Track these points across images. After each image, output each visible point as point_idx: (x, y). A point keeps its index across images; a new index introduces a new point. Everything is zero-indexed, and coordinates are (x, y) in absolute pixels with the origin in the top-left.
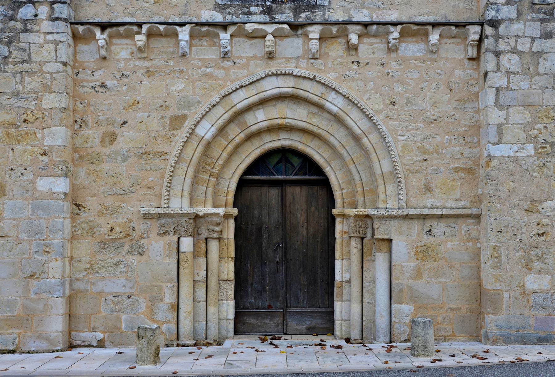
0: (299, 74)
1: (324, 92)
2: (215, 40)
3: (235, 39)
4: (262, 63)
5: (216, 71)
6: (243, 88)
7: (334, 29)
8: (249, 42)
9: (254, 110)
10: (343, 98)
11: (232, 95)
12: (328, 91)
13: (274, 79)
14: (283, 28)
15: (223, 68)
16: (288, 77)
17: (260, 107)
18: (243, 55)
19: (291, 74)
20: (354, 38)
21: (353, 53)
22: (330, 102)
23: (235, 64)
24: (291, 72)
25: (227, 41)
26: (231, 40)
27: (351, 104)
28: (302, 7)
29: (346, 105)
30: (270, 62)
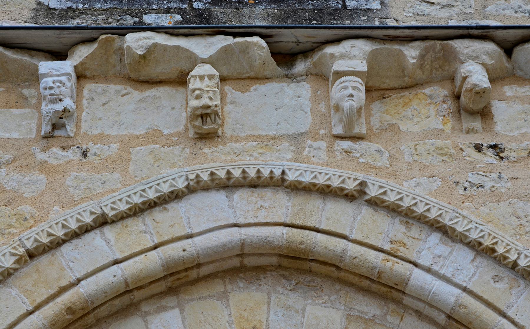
0: (307, 179)
1: (399, 237)
2: (26, 92)
3: (89, 87)
4: (180, 152)
5: (16, 176)
6: (107, 229)
7: (411, 53)
8: (136, 94)
9: (147, 313)
10: (469, 254)
11: (66, 249)
12: (415, 230)
13: (219, 198)
14: (245, 49)
15: (44, 167)
16: (268, 193)
17: (170, 301)
19: (279, 183)
20: (476, 75)
21: (477, 124)
22: (428, 270)
23: (85, 155)
24: (277, 173)
25: (64, 79)
26: (79, 87)
27: (505, 273)
28: (301, 13)
29: (488, 277)
30: (206, 150)
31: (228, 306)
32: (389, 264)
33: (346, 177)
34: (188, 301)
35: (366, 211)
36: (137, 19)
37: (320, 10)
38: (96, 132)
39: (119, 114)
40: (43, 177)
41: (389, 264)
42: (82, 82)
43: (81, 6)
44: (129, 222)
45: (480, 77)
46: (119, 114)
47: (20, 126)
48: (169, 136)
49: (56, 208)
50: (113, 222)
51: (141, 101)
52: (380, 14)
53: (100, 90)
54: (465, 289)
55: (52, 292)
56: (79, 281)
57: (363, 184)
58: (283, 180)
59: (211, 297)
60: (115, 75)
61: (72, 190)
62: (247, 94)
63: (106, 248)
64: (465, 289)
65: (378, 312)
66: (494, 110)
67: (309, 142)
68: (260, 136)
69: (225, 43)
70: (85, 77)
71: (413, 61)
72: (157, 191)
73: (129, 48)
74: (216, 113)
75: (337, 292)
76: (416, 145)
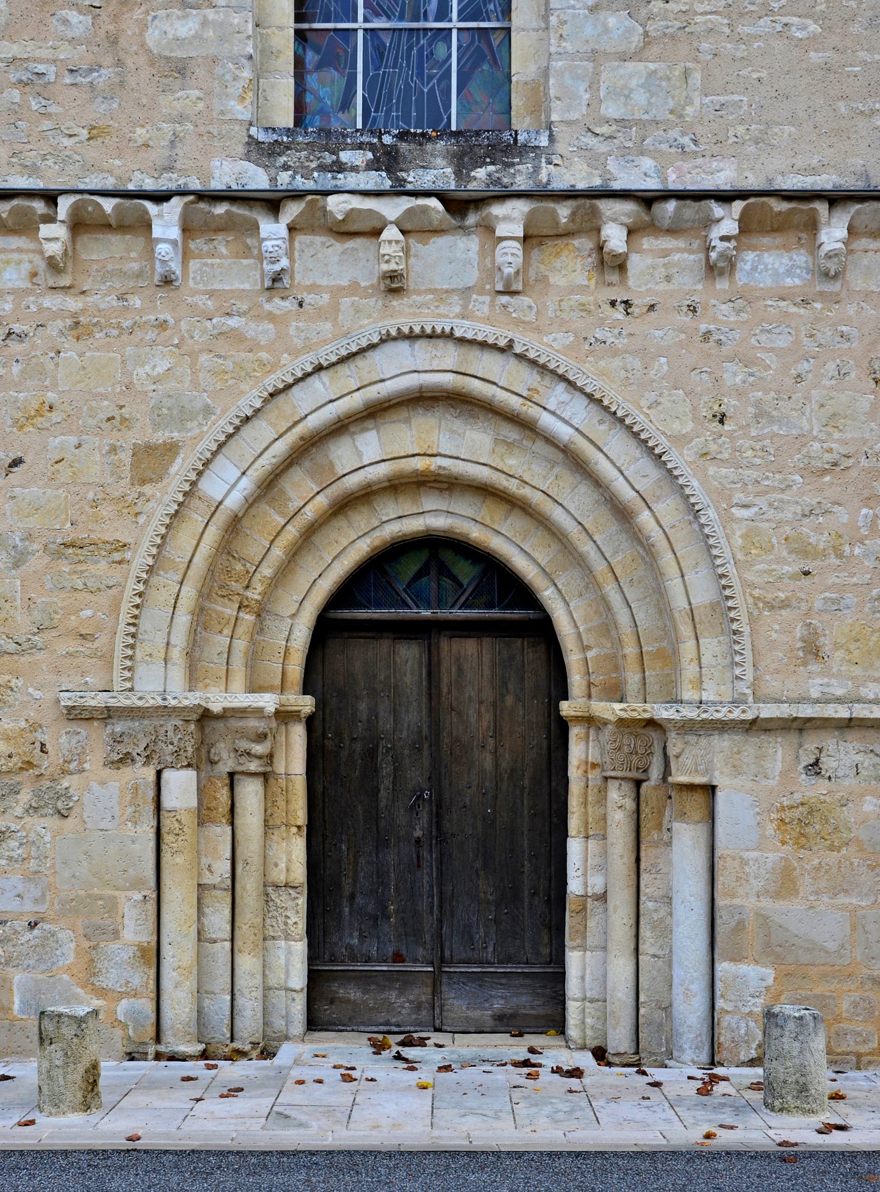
0: (469, 336)
1: (535, 385)
2: (249, 241)
3: (301, 239)
4: (374, 303)
5: (253, 325)
6: (323, 374)
7: (564, 211)
8: (339, 246)
9: (354, 433)
10: (585, 401)
11: (295, 390)
12: (547, 381)
13: (403, 347)
14: (425, 209)
15: (271, 317)
16: (440, 343)
17: (370, 423)
18: (324, 282)
19: (448, 336)
20: (615, 237)
21: (614, 278)
22: (553, 413)
23: (301, 305)
24: (447, 330)
25: (279, 242)
26: (291, 240)
27: (608, 418)
28: (476, 149)
29: (595, 421)
30: (395, 303)
31: (411, 429)
32: (525, 408)
33: (498, 334)
34: (383, 424)
35: (513, 361)
36: (334, 157)
37: (493, 146)
38: (308, 283)
39: (326, 265)
40: (271, 326)
41: (525, 408)
42: (294, 233)
43: (285, 139)
44: (339, 368)
45: (618, 243)
46: (326, 265)
47: (249, 277)
48: (366, 288)
49: (285, 355)
50: (327, 368)
51: (343, 253)
52: (547, 151)
53: (308, 242)
54: (577, 429)
55: (289, 425)
56: (306, 416)
57: (511, 341)
58: (452, 334)
59: (399, 421)
60: (320, 226)
61: (295, 339)
62: (427, 247)
63: (323, 390)
64: (577, 429)
65: (517, 437)
66: (629, 265)
67: (474, 296)
68: (436, 290)
69: (409, 205)
70: (295, 229)
71: (564, 220)
72: (358, 344)
73: (331, 212)
74: (402, 275)
75: (489, 420)
76: (561, 301)
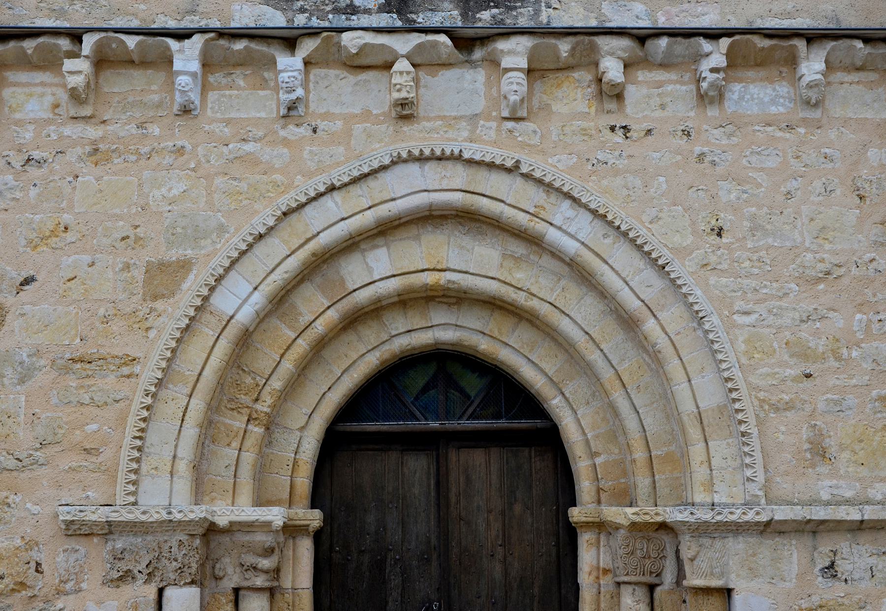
0: (477, 157)
2: (266, 74)
3: (315, 72)
4: (386, 129)
5: (268, 150)
7: (564, 47)
9: (364, 250)
10: (590, 217)
11: (308, 209)
12: (553, 198)
14: (435, 44)
15: (285, 142)
16: (449, 165)
17: (380, 241)
18: (337, 110)
19: (457, 158)
20: (612, 69)
21: (612, 105)
22: (560, 228)
23: (315, 131)
24: (456, 152)
25: (295, 74)
26: (307, 73)
27: (612, 232)
29: (600, 235)
30: (405, 129)
31: (420, 246)
34: (393, 241)
35: (519, 181)
38: (323, 111)
39: (340, 95)
40: (286, 150)
41: (533, 224)
42: (309, 68)
44: (351, 188)
46: (340, 95)
48: (377, 115)
49: (299, 177)
50: (339, 188)
51: (356, 84)
53: (323, 74)
54: (583, 243)
55: (301, 242)
56: (319, 233)
57: (518, 162)
58: (461, 156)
59: (409, 238)
61: (309, 163)
62: (436, 78)
63: (335, 208)
64: (583, 243)
65: (524, 252)
66: (626, 94)
67: (482, 122)
68: (445, 117)
70: (311, 63)
71: (565, 55)
72: (370, 166)
74: (412, 103)
76: (564, 126)
